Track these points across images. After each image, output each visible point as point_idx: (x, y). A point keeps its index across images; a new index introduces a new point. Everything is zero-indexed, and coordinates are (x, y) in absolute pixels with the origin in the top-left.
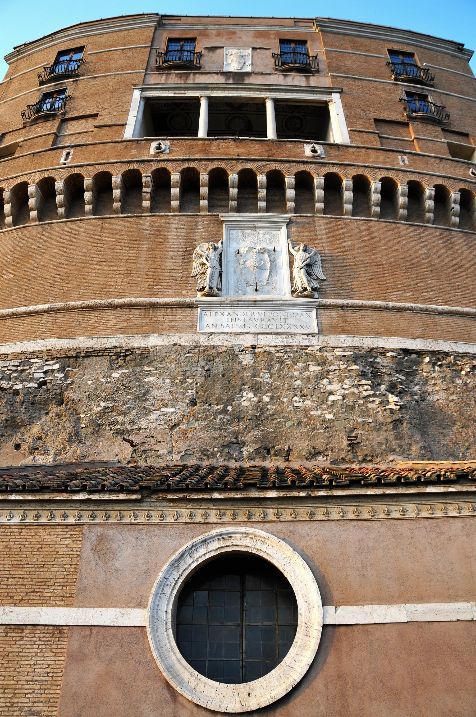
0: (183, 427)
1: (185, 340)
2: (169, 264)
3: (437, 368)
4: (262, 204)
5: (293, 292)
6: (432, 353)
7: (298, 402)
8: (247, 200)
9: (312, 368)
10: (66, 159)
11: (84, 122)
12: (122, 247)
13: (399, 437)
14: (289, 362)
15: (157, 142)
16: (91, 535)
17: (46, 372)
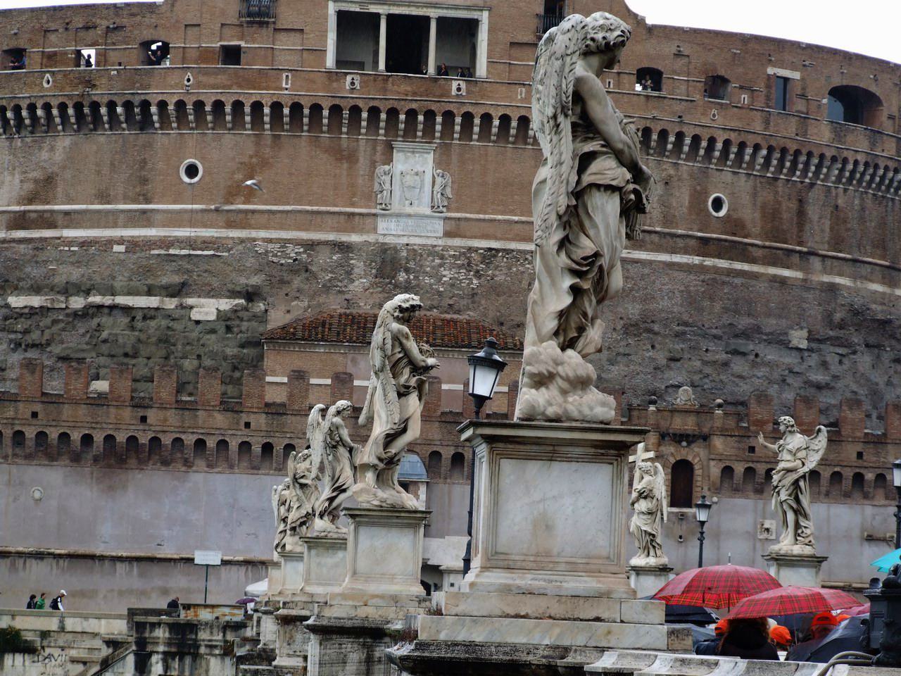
0: (371, 291)
1: (371, 238)
2: (360, 181)
3: (505, 260)
4: (420, 134)
5: (433, 207)
6: (504, 250)
7: (427, 280)
8: (410, 133)
9: (436, 261)
10: (287, 84)
11: (292, 34)
12: (331, 165)
13: (473, 302)
14: (425, 256)
15: (351, 76)
16: (350, 356)
17: (296, 253)
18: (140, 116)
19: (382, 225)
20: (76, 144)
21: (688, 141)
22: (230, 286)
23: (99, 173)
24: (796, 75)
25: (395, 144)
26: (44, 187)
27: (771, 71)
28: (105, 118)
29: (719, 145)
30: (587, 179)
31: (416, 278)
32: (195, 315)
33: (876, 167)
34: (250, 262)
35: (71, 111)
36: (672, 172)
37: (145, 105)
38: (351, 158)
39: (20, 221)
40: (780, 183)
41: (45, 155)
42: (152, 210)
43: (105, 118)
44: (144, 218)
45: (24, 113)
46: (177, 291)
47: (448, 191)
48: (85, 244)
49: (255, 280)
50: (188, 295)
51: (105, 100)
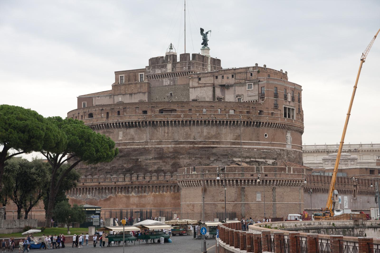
7: (291, 156)
18: (258, 124)
19: (287, 146)
22: (273, 157)
23: (249, 135)
25: (288, 131)
26: (239, 137)
32: (268, 163)
34: (275, 153)
37: (260, 123)
39: (234, 143)
41: (238, 131)
44: (259, 144)
46: (264, 158)
48: (248, 149)
49: (276, 156)
51: (253, 121)
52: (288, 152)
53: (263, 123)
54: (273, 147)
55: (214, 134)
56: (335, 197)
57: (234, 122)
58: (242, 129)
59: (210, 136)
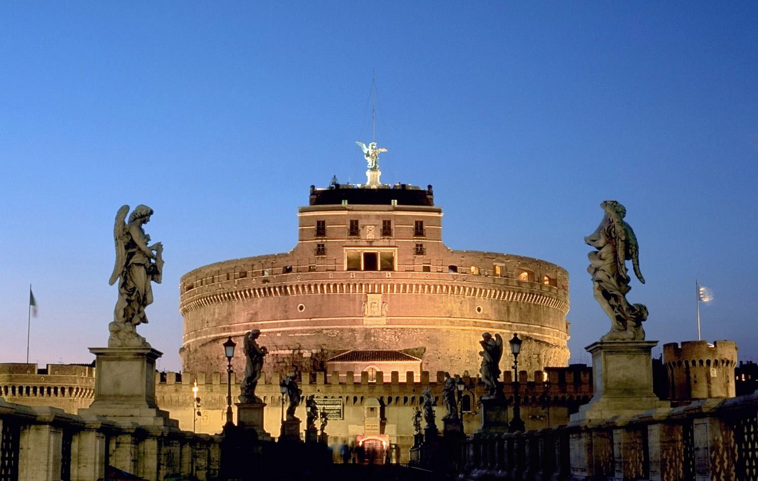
1: (361, 326)
7: (381, 339)
18: (284, 290)
20: (264, 301)
21: (467, 289)
23: (271, 310)
24: (504, 265)
26: (254, 317)
27: (494, 264)
28: (273, 292)
29: (478, 290)
30: (131, 261)
31: (377, 339)
33: (533, 294)
35: (262, 291)
36: (463, 299)
37: (285, 287)
38: (354, 300)
40: (500, 302)
41: (254, 305)
42: (289, 322)
43: (273, 292)
44: (287, 325)
45: (247, 292)
47: (387, 309)
50: (303, 349)
51: (273, 286)
52: (367, 334)
53: (291, 287)
54: (315, 328)
55: (225, 314)
56: (366, 411)
57: (245, 291)
58: (260, 300)
59: (220, 319)
